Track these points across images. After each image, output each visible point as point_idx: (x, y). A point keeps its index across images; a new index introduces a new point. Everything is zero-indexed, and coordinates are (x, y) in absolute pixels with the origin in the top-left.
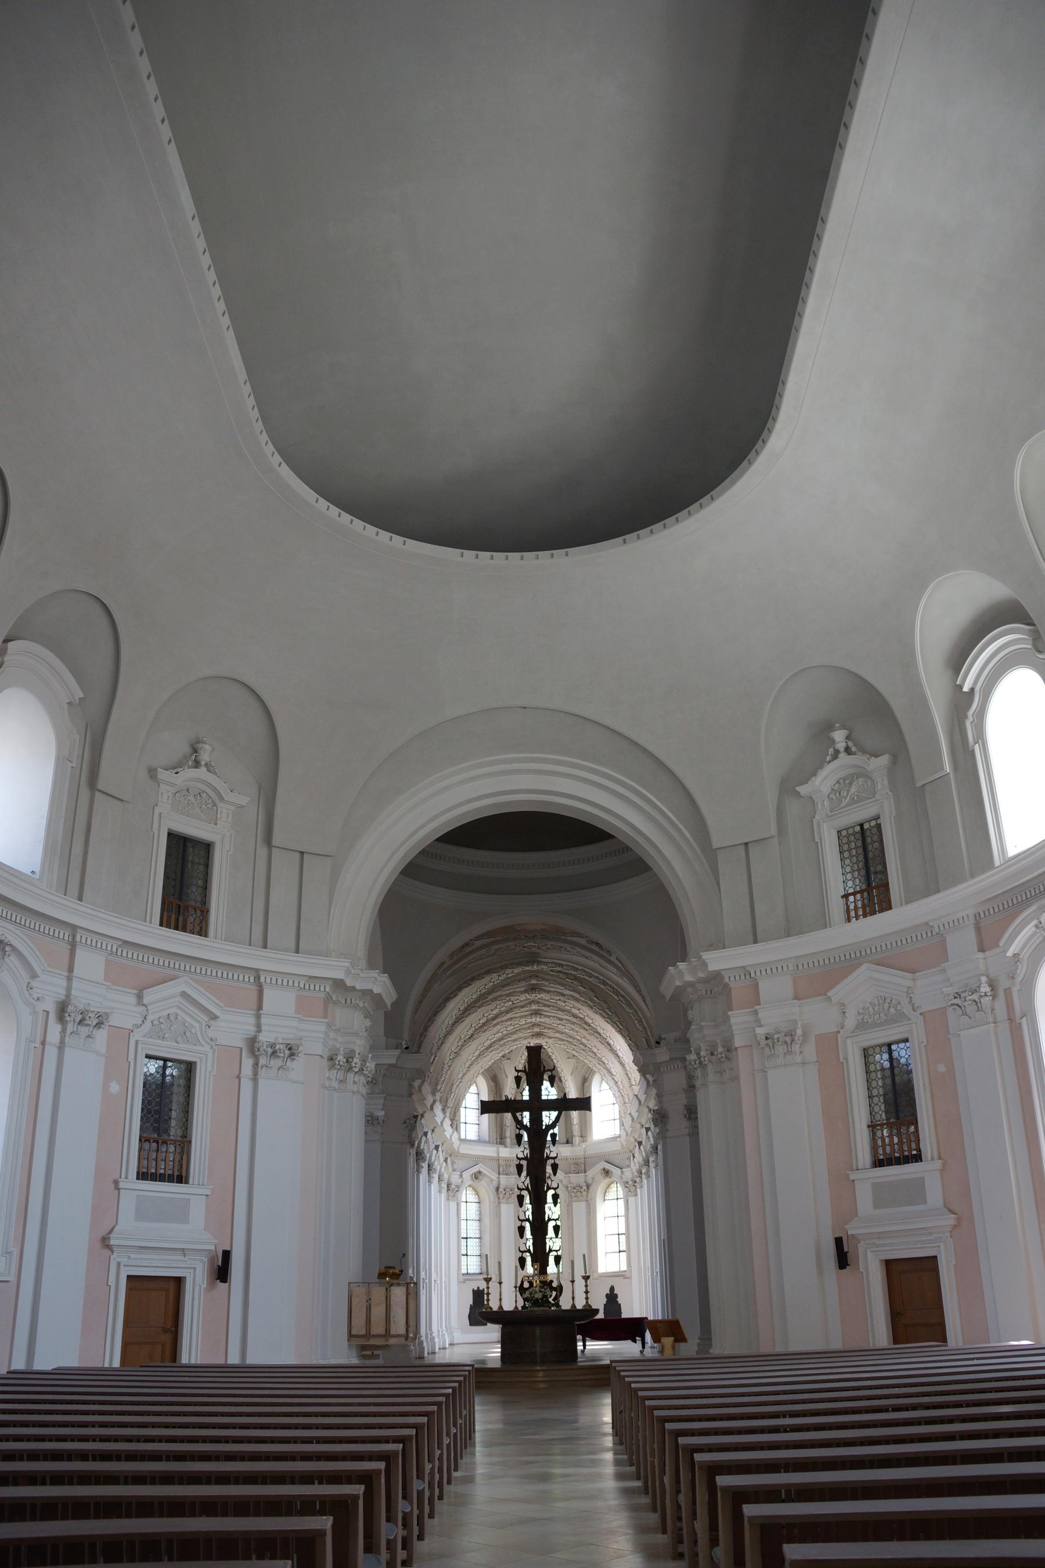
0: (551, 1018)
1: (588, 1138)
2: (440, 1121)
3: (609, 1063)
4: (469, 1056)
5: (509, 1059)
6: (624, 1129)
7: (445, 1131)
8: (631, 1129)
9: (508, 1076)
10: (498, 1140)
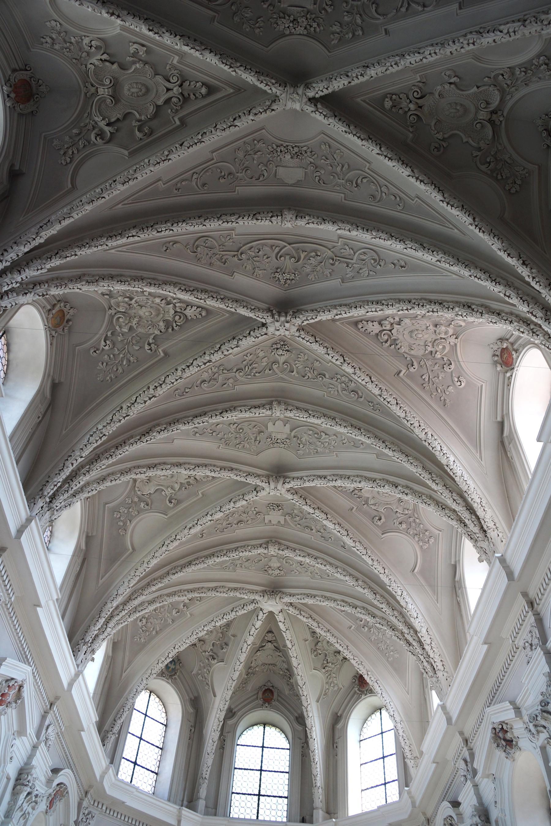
0: (305, 478)
1: (340, 813)
2: (19, 525)
3: (405, 593)
4: (146, 556)
5: (222, 661)
6: (409, 792)
7: (39, 605)
8: (486, 646)
9: (217, 695)
10: (185, 803)
